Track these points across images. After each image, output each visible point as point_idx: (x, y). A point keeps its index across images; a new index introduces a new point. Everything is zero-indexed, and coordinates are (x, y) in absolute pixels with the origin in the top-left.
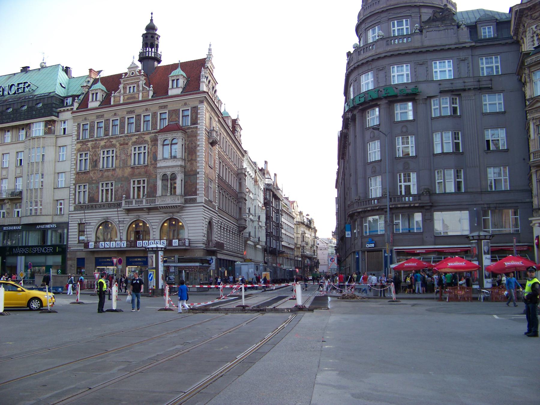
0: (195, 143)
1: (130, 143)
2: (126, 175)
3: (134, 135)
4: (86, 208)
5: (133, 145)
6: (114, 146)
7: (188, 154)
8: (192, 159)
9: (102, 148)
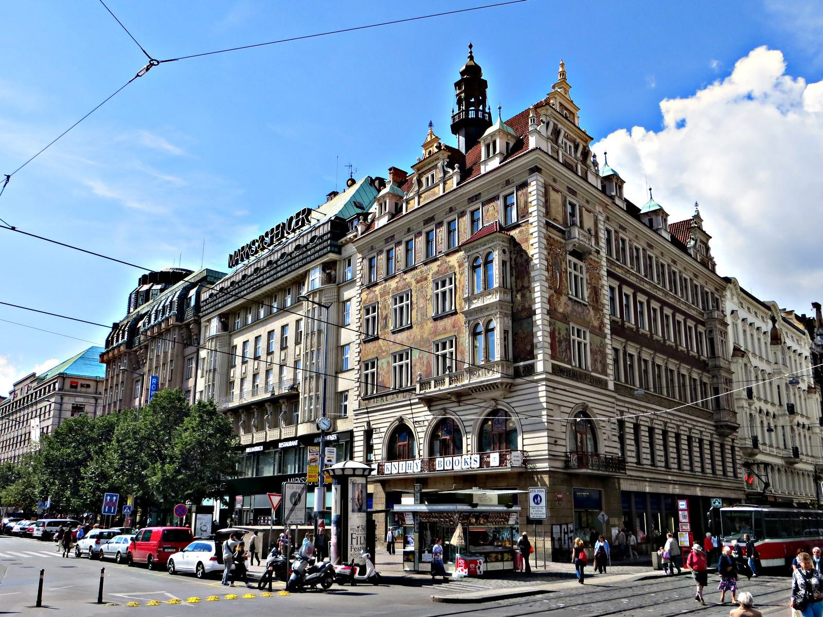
2: (425, 336)
8: (523, 286)
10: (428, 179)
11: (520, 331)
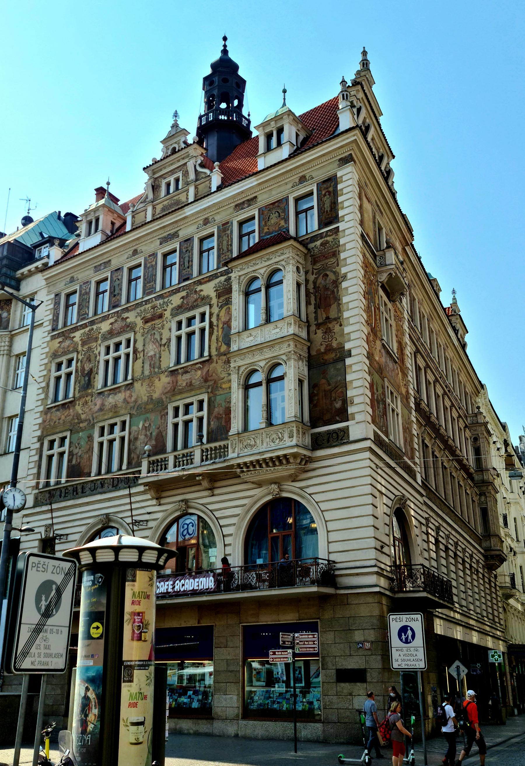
0: (335, 273)
1: (167, 314)
2: (156, 396)
3: (178, 291)
4: (60, 496)
5: (173, 315)
6: (130, 327)
7: (317, 307)
8: (328, 318)
9: (105, 338)
10: (168, 185)
11: (324, 381)
